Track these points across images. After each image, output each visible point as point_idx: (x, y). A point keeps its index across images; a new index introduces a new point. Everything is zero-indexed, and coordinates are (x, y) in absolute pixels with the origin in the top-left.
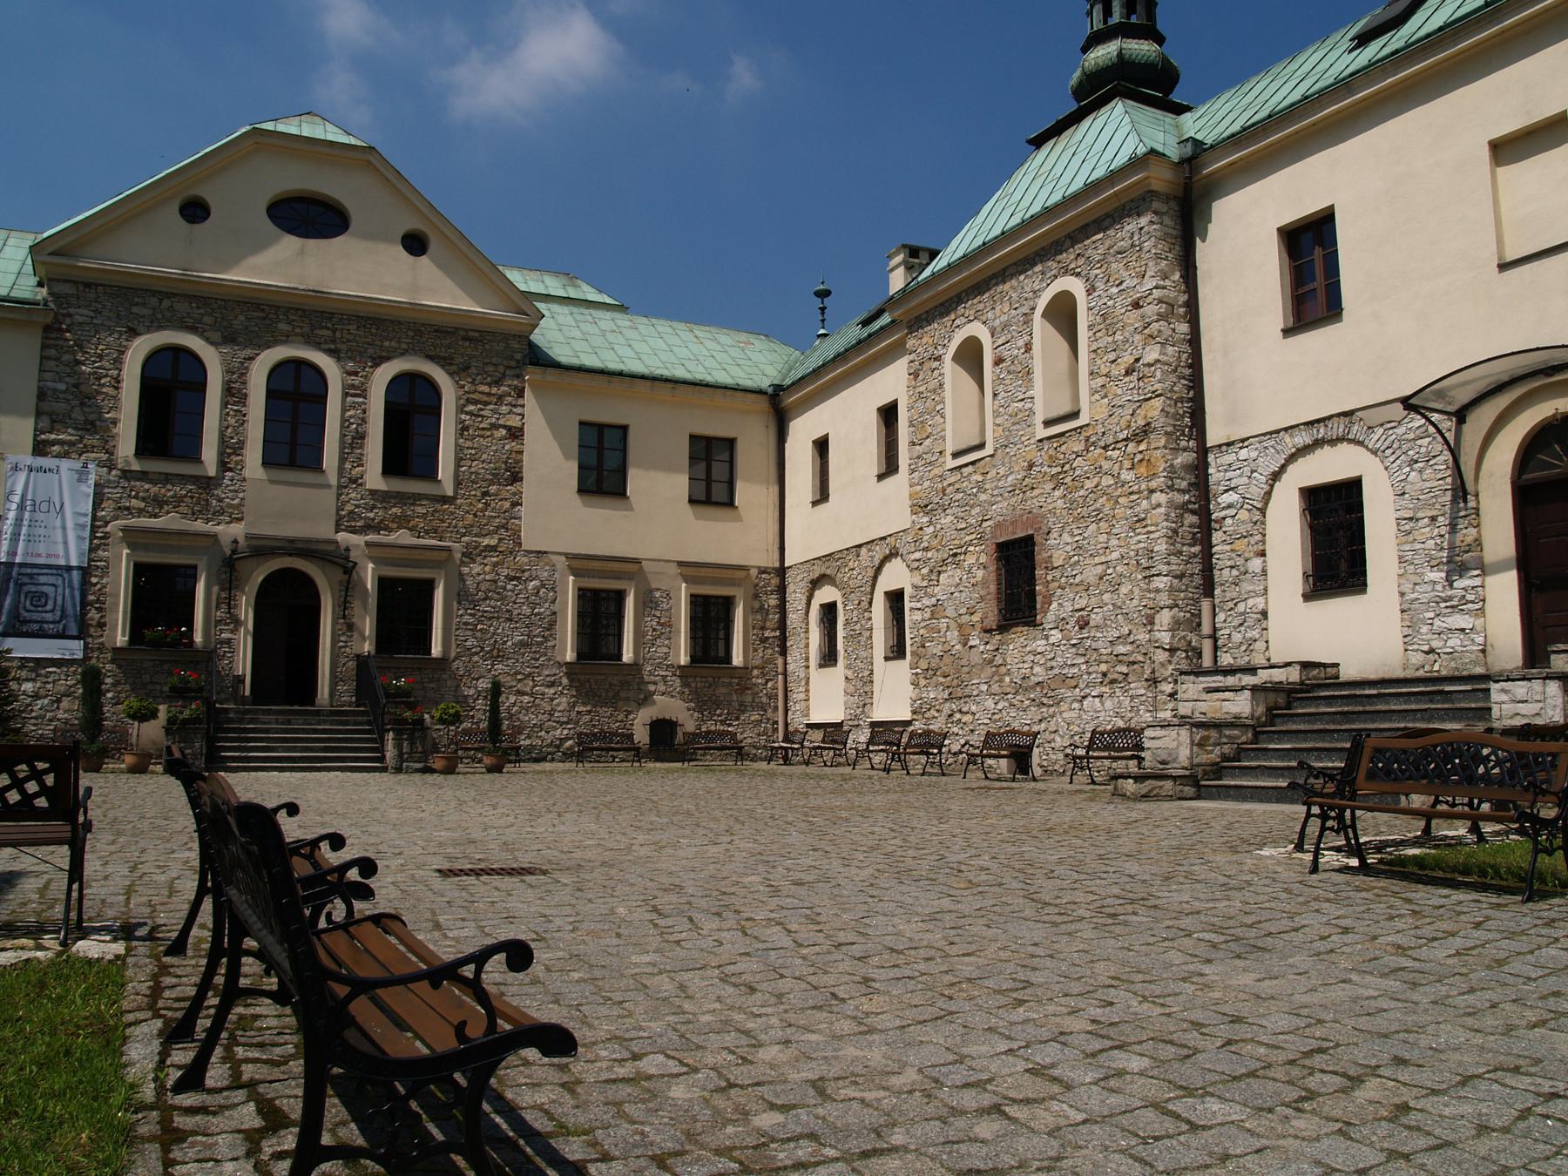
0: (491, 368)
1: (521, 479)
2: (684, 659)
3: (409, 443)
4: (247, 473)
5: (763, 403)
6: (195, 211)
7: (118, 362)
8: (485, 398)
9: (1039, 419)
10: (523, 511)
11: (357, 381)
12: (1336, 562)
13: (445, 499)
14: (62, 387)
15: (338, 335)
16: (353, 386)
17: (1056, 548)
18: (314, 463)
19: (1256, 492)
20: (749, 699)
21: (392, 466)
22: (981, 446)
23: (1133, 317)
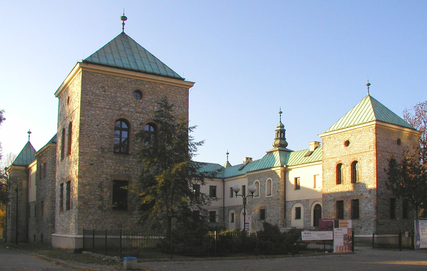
5: (221, 180)
9: (266, 195)
12: (298, 216)
17: (268, 211)
19: (291, 207)
22: (258, 196)
23: (278, 185)
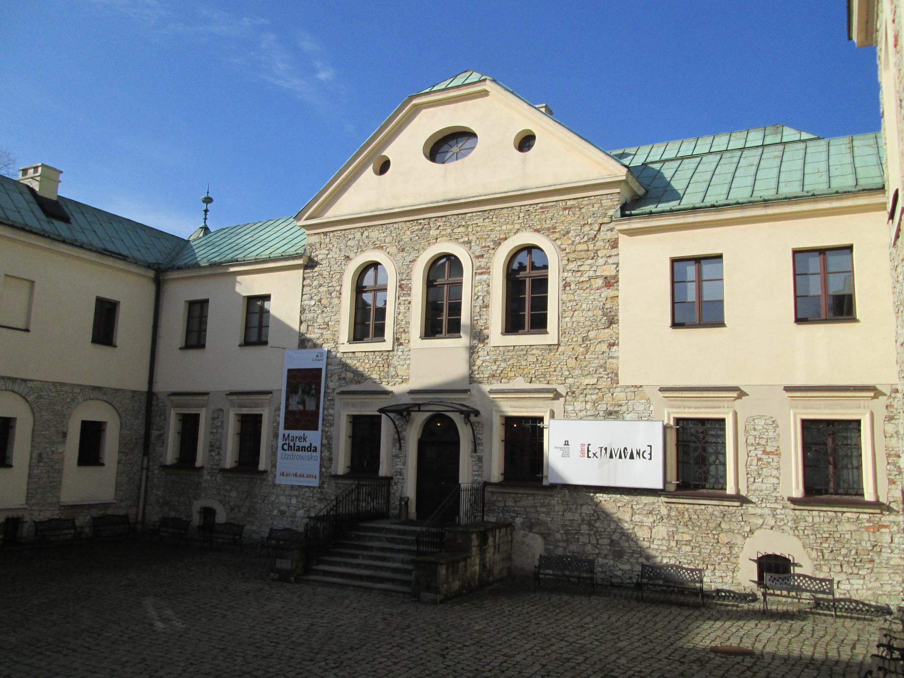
0: (587, 228)
1: (617, 322)
2: (798, 492)
3: (526, 302)
4: (412, 345)
7: (340, 280)
8: (583, 255)
10: (621, 351)
11: (482, 262)
14: (313, 303)
15: (470, 229)
16: (480, 267)
20: (887, 538)
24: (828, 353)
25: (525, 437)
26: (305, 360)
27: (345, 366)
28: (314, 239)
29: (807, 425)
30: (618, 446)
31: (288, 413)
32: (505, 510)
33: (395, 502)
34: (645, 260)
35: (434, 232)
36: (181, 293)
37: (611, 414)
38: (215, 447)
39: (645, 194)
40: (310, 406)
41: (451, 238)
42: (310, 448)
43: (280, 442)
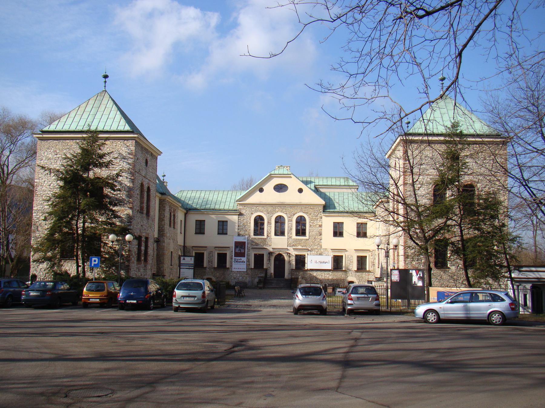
2: (356, 269)
6: (261, 190)
7: (250, 219)
11: (290, 219)
13: (307, 240)
18: (282, 234)
21: (298, 234)
24: (362, 243)
25: (300, 261)
26: (240, 239)
27: (253, 241)
28: (241, 207)
29: (358, 257)
30: (322, 261)
31: (235, 253)
32: (296, 275)
33: (268, 274)
34: (328, 223)
35: (277, 210)
36: (193, 218)
37: (320, 254)
38: (210, 262)
39: (328, 207)
40: (242, 251)
41: (282, 211)
42: (243, 262)
43: (233, 260)
